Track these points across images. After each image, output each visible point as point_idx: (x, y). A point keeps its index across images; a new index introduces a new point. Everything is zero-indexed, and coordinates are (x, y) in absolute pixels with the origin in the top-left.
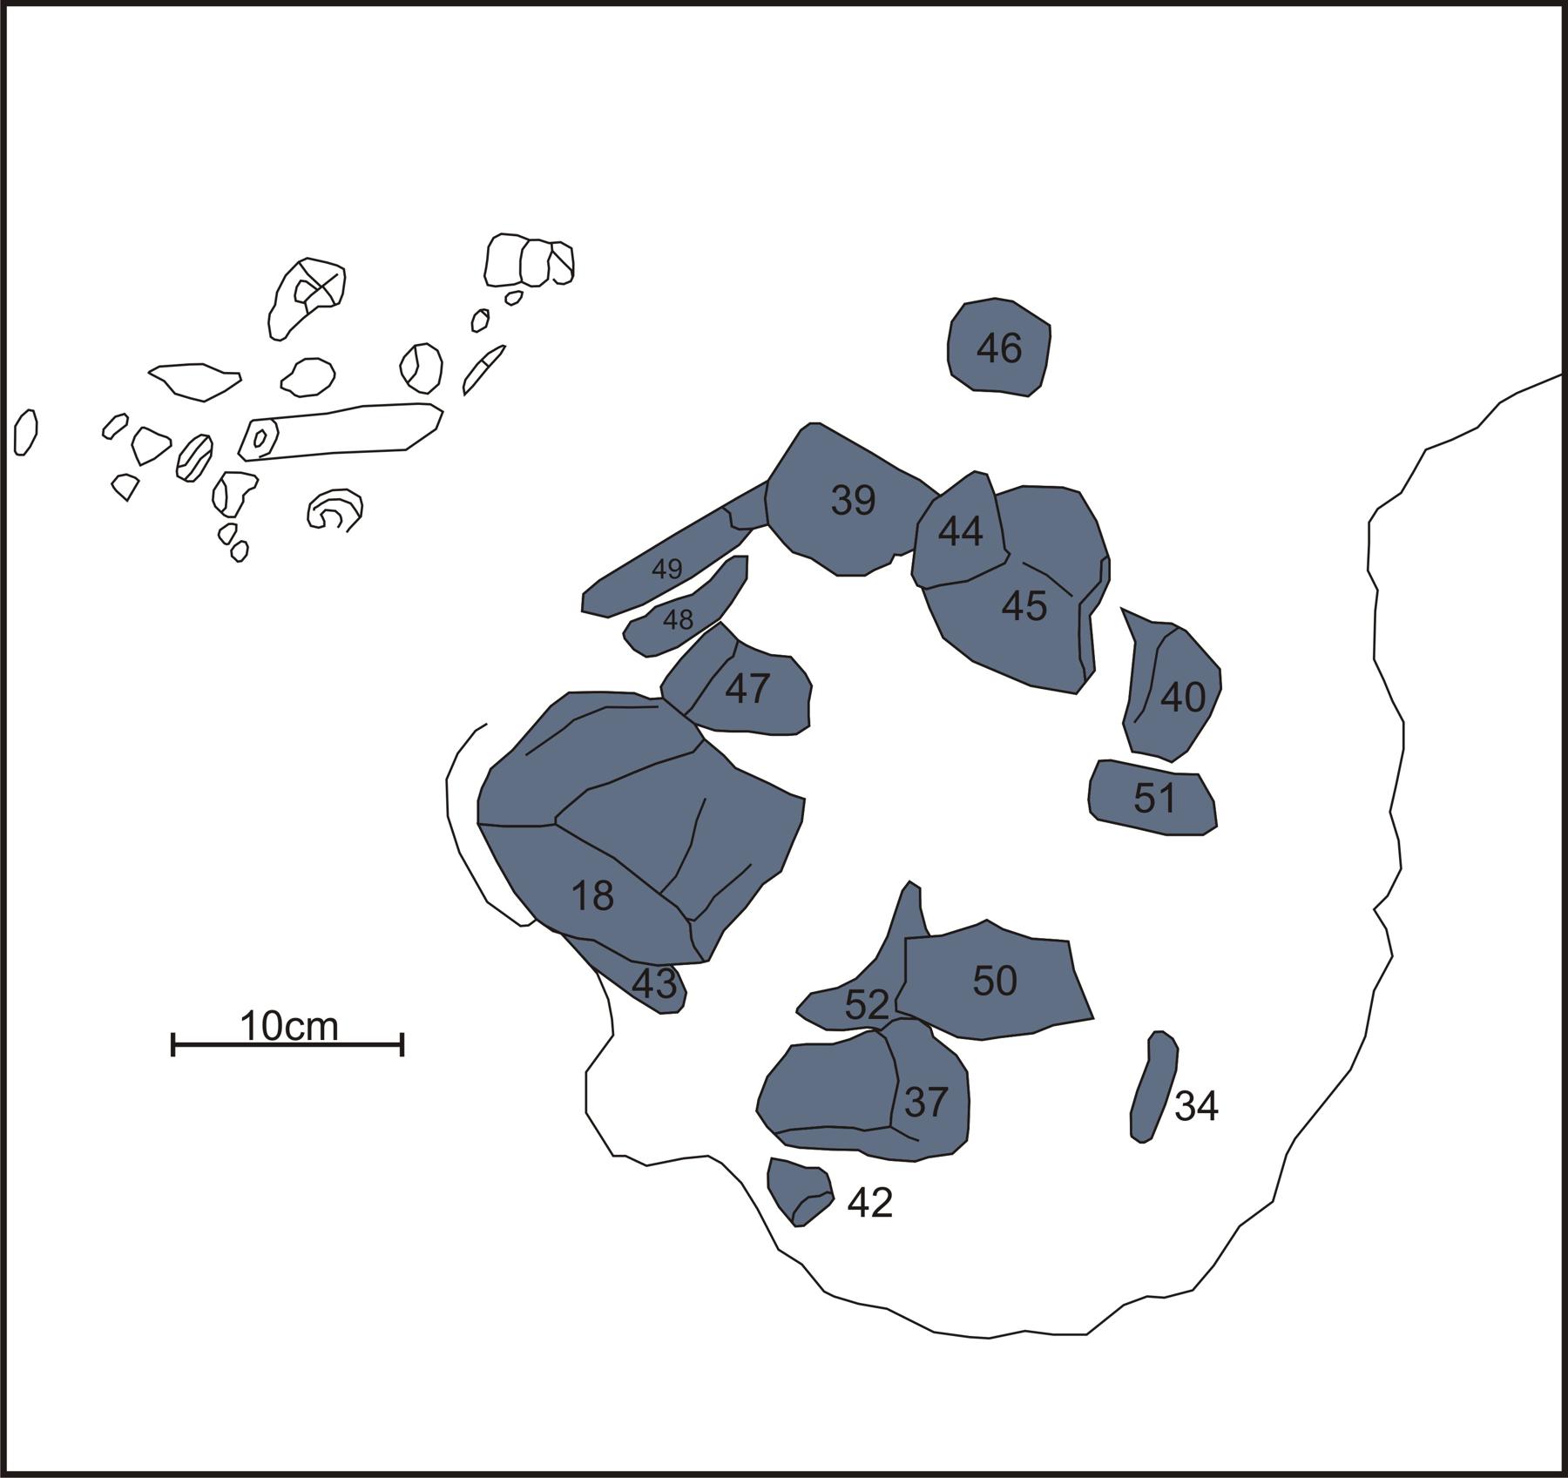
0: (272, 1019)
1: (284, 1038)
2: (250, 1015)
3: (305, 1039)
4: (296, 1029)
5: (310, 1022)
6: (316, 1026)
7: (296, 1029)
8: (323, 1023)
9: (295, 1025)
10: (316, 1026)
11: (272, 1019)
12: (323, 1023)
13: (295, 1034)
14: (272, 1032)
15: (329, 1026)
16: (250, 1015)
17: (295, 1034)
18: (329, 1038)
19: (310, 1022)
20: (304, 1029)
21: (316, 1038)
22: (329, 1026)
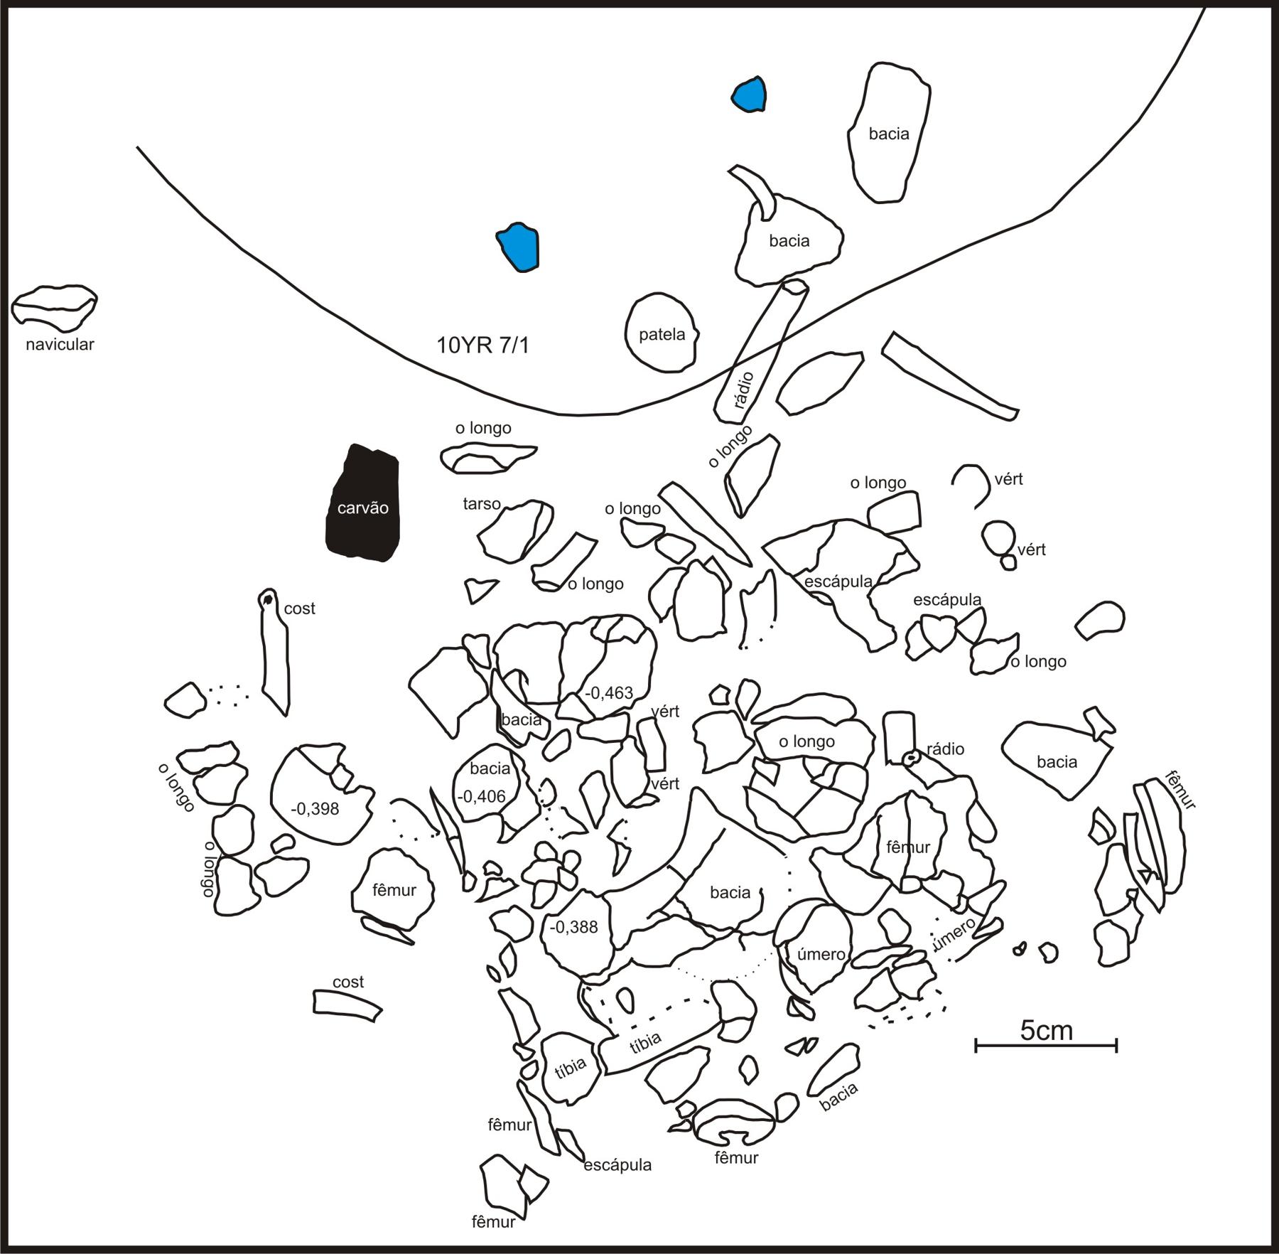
1: (1036, 1040)
3: (1049, 1041)
4: (1044, 1032)
5: (1054, 1028)
6: (1058, 1030)
7: (1044, 1032)
8: (1062, 1028)
9: (1043, 1029)
10: (1058, 1030)
12: (1062, 1028)
13: (1043, 1036)
15: (1066, 1030)
17: (1043, 1036)
18: (1066, 1041)
19: (1054, 1028)
20: (1050, 1032)
21: (1058, 1041)
22: (1066, 1030)
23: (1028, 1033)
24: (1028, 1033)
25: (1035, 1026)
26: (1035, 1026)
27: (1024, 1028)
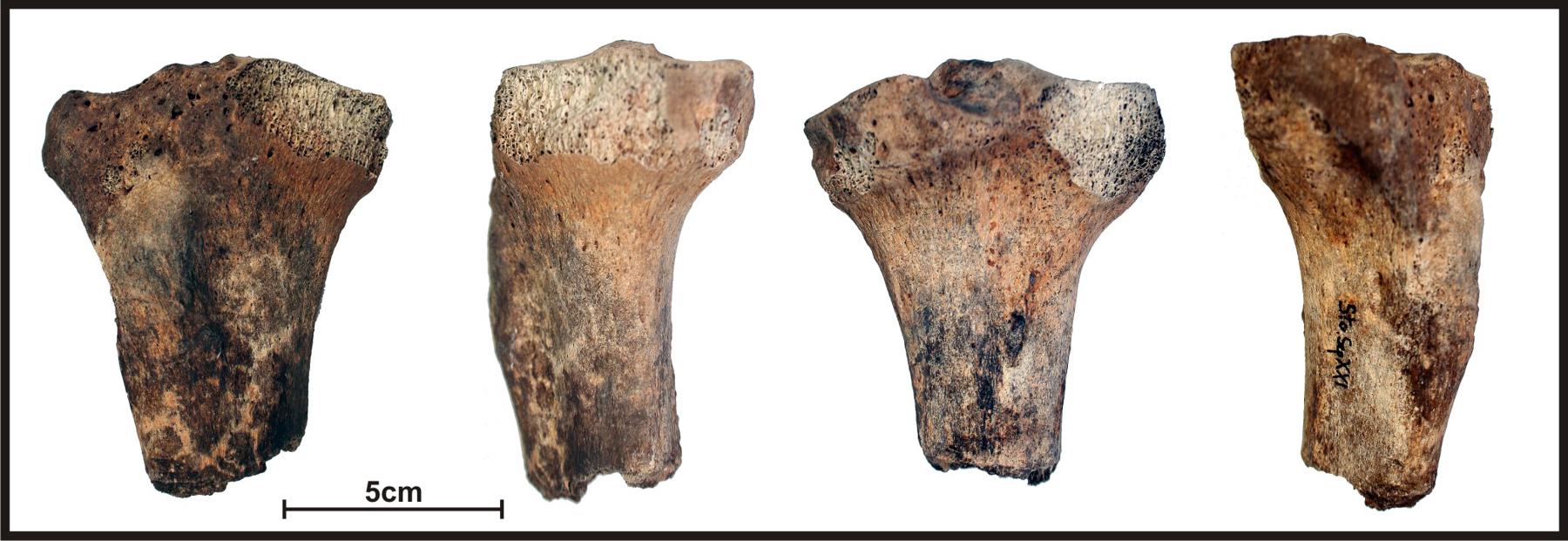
3: (396, 504)
4: (389, 494)
6: (405, 493)
7: (389, 494)
10: (405, 493)
15: (415, 493)
18: (415, 504)
19: (401, 490)
20: (396, 494)
21: (405, 504)
22: (415, 493)
23: (372, 495)
24: (372, 495)
25: (380, 488)
26: (380, 488)
27: (369, 490)
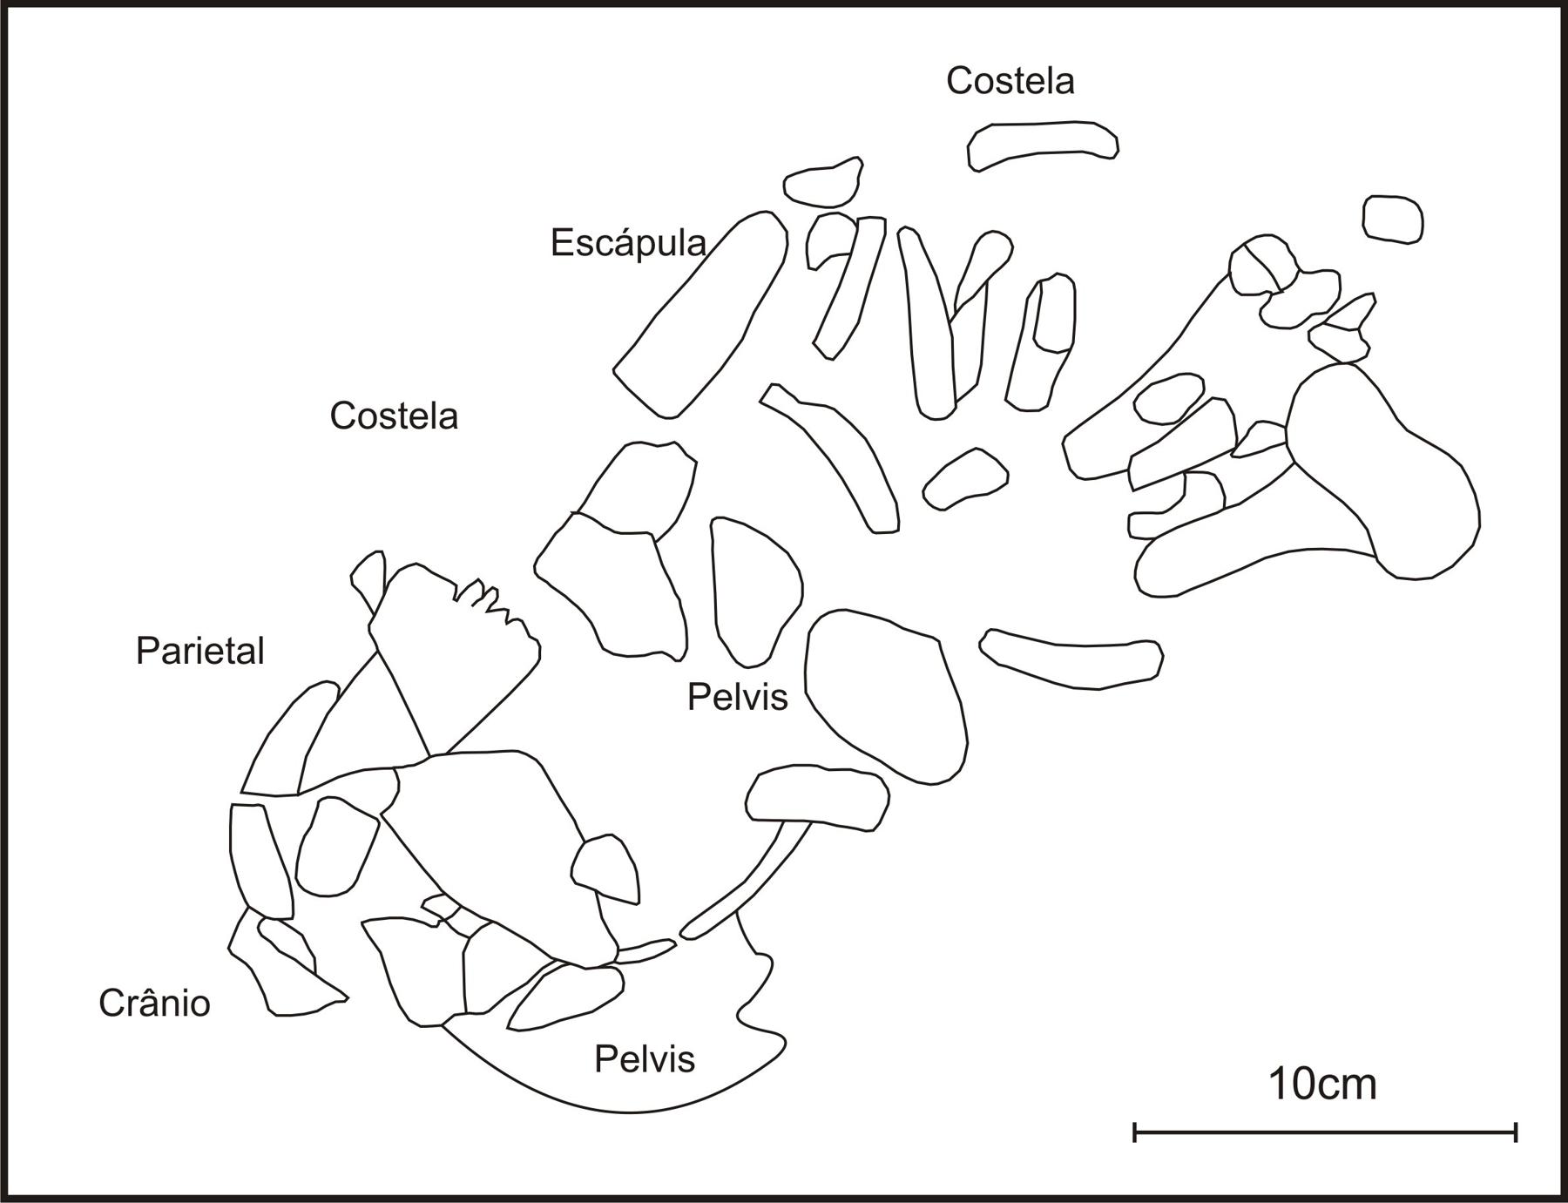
0: (1304, 1077)
2: (1280, 1071)
5: (1346, 1079)
6: (1352, 1083)
8: (1359, 1080)
9: (1329, 1082)
10: (1352, 1083)
11: (1304, 1077)
12: (1359, 1080)
13: (1329, 1091)
14: (1304, 1091)
15: (1366, 1083)
16: (1280, 1071)
17: (1329, 1091)
19: (1346, 1079)
22: (1366, 1083)
